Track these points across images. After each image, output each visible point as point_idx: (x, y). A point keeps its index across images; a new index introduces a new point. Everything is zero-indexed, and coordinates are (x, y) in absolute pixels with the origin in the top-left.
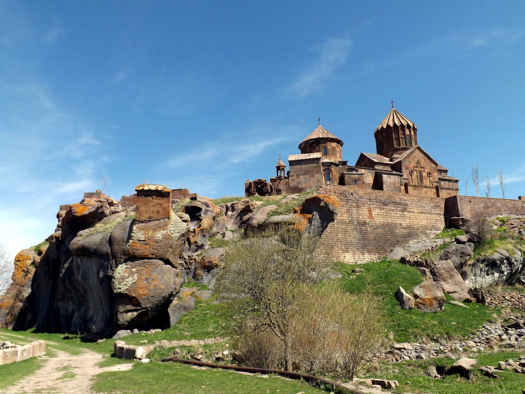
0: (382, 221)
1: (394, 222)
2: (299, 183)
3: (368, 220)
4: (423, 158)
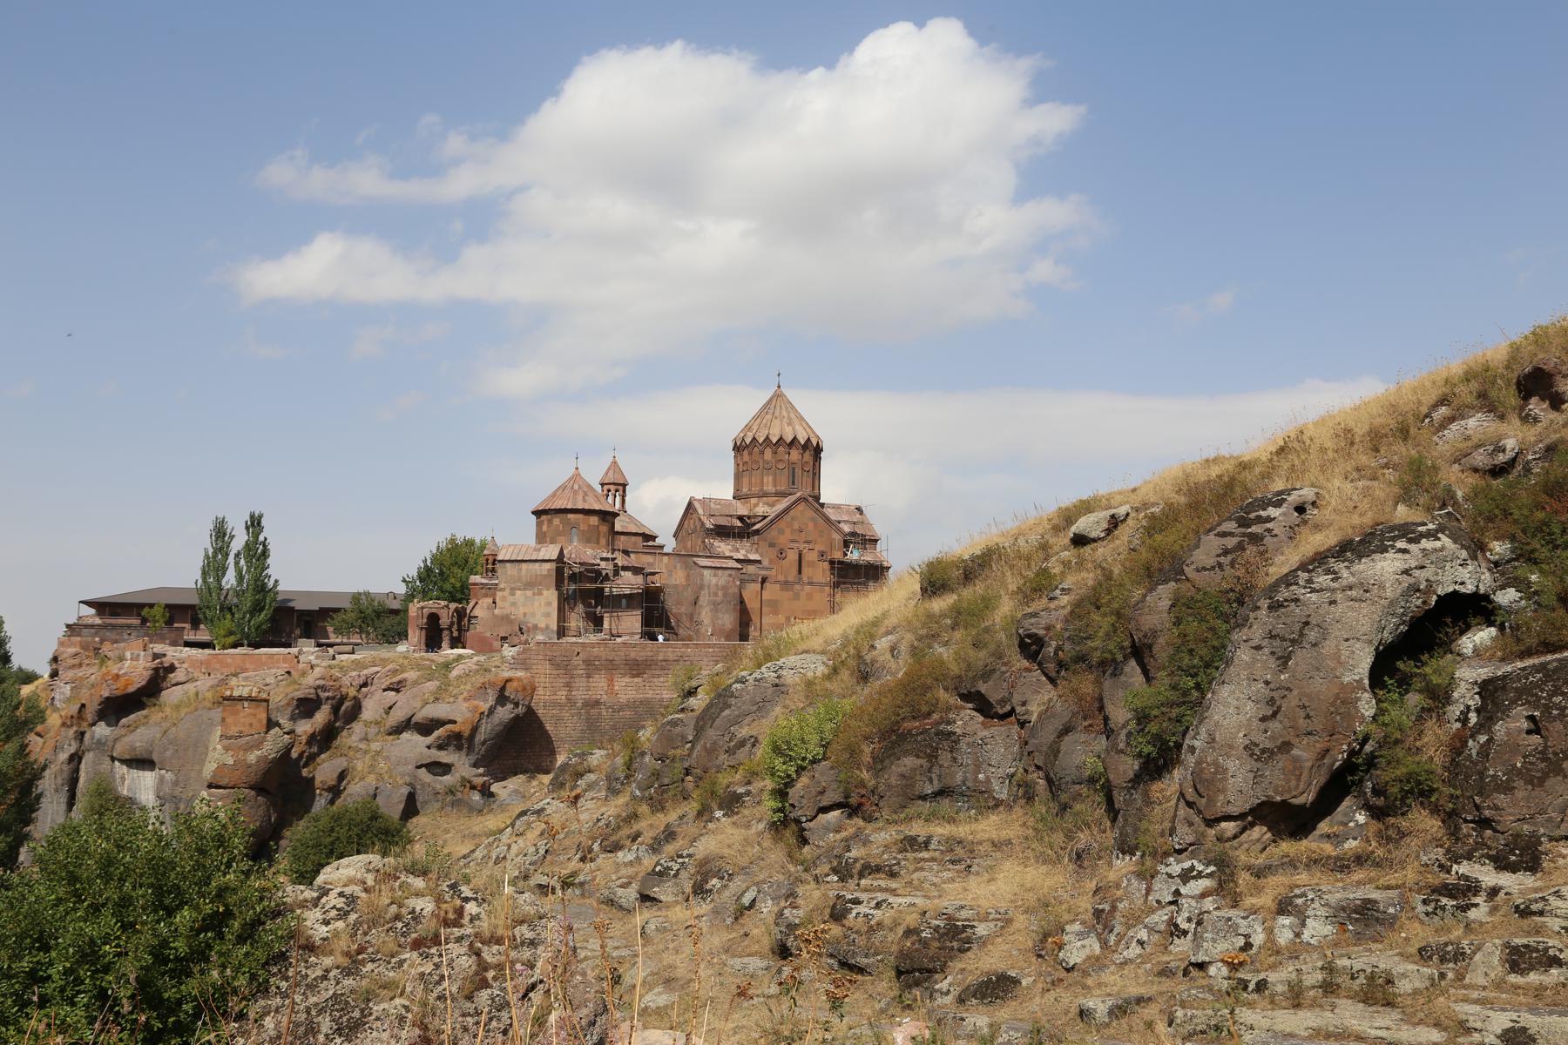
4: (813, 519)
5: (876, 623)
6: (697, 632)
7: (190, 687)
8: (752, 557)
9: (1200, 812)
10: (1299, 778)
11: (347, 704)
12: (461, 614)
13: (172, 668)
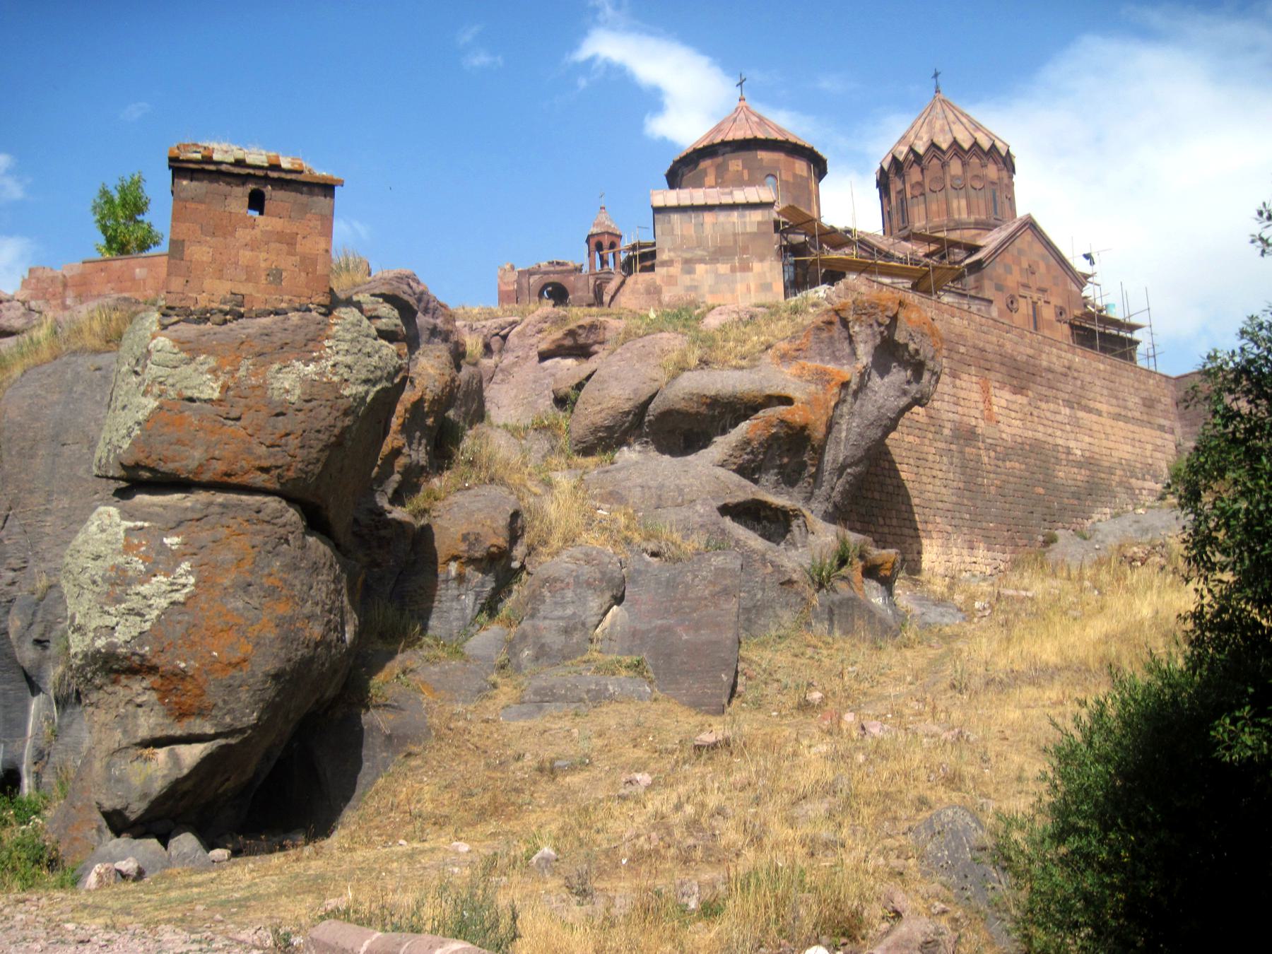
0: (1019, 432)
1: (1050, 439)
2: (694, 288)
3: (982, 423)
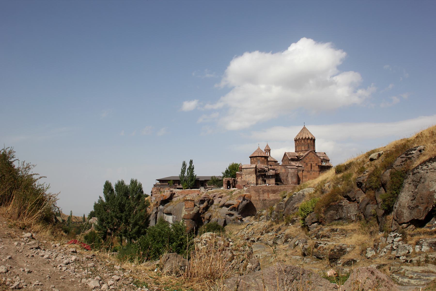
5: (325, 180)
6: (288, 183)
7: (178, 198)
8: (300, 165)
9: (398, 222)
10: (420, 214)
11: (211, 201)
12: (234, 180)
13: (174, 194)
